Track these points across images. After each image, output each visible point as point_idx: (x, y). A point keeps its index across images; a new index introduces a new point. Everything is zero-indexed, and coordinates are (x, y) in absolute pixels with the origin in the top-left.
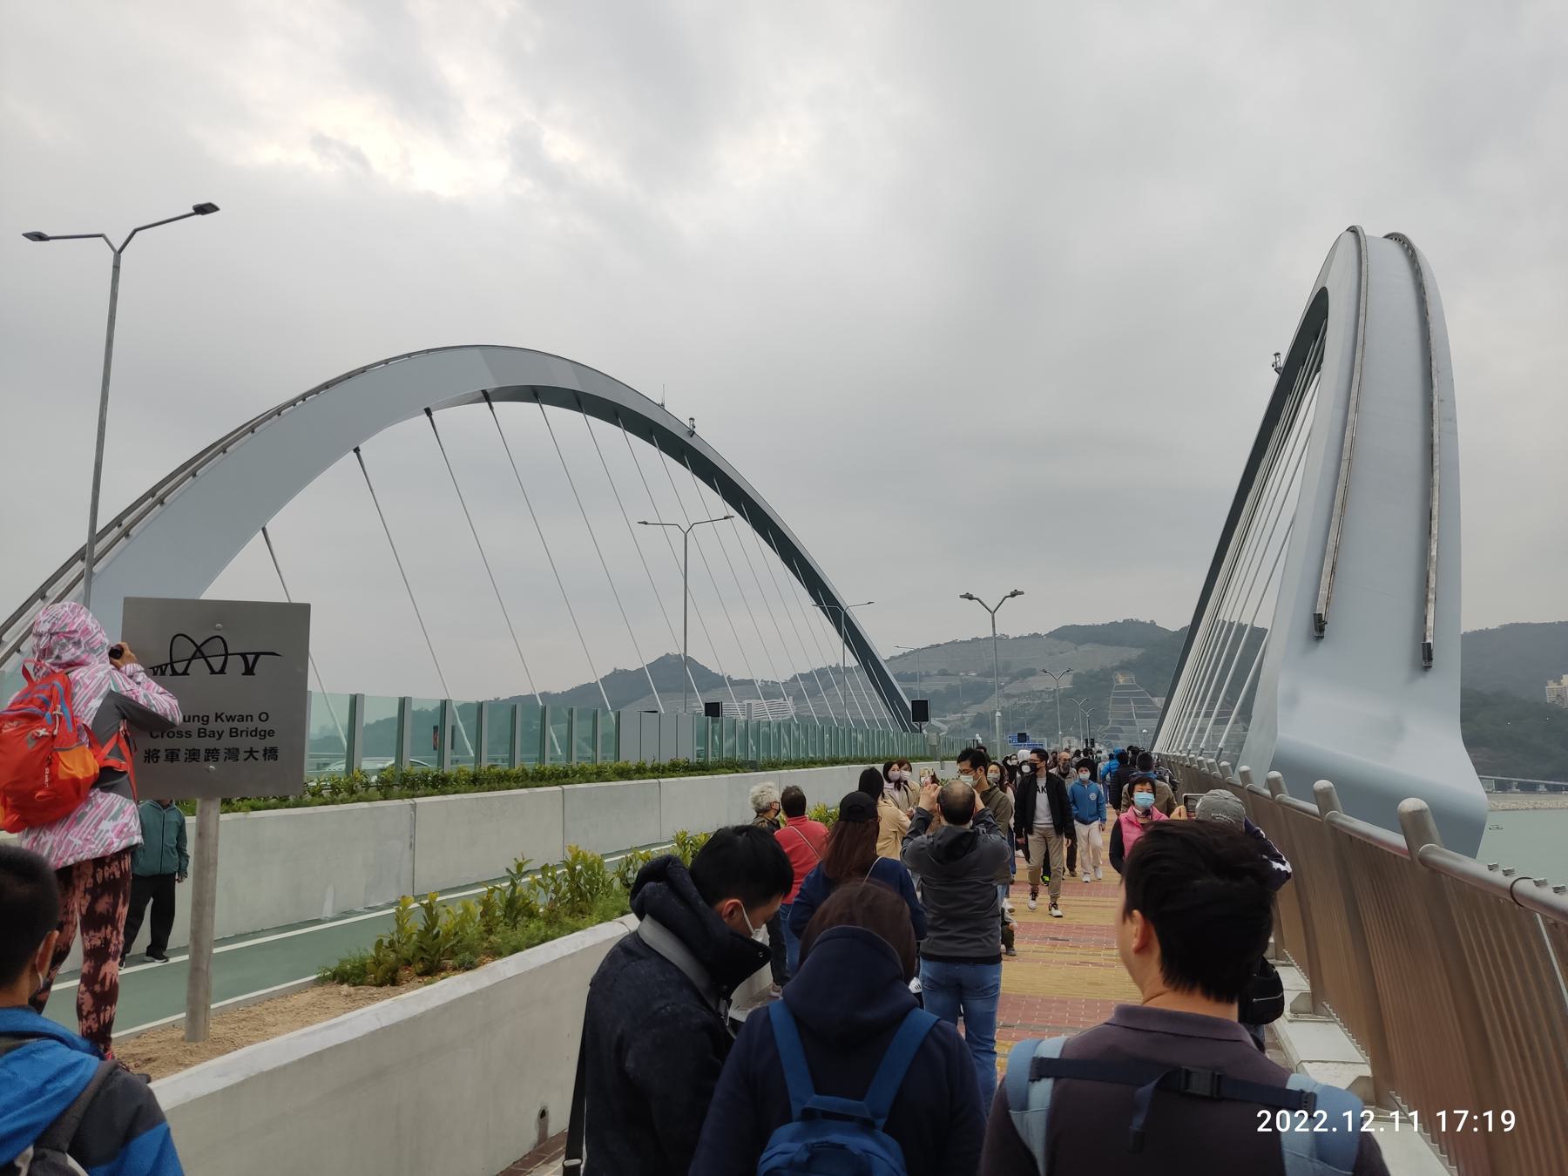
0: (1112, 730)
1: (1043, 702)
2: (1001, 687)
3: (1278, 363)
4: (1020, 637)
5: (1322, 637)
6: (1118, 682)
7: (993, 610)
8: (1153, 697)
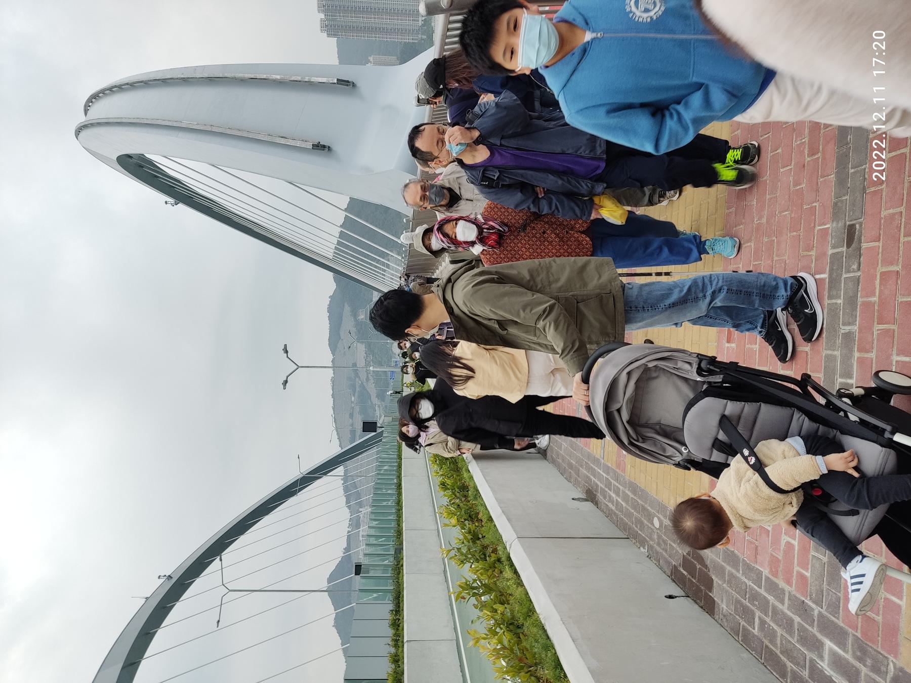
2: (362, 382)
3: (172, 203)
5: (329, 147)
6: (363, 318)
7: (296, 367)
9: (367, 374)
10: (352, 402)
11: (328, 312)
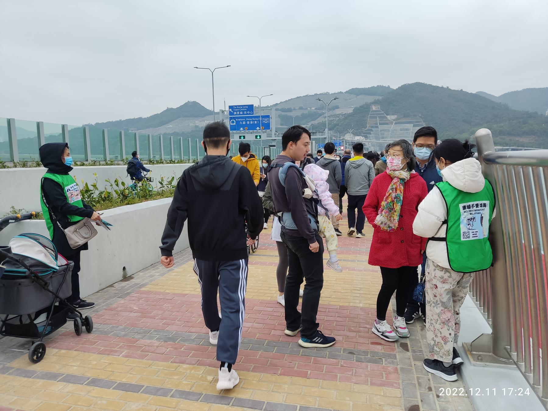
0: (369, 130)
1: (340, 119)
6: (373, 109)
8: (387, 115)
9: (329, 116)
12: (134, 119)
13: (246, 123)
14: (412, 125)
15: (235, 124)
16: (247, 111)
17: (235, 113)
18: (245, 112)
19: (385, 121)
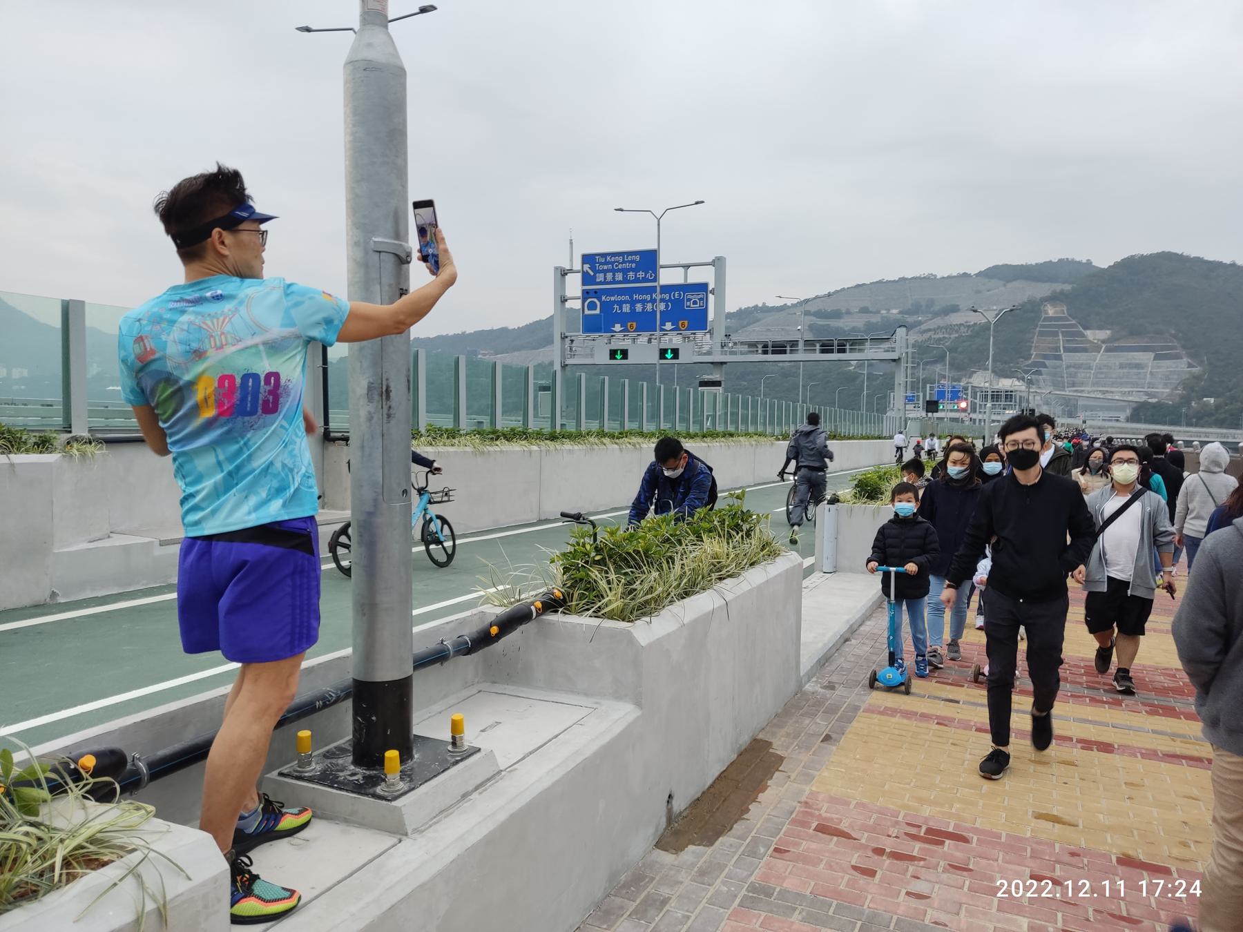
0: (1035, 364)
1: (960, 336)
4: (949, 277)
6: (1047, 313)
8: (1085, 329)
10: (888, 310)
11: (1060, 260)
12: (492, 331)
13: (633, 310)
14: (1152, 355)
15: (597, 311)
16: (635, 270)
17: (600, 277)
18: (631, 274)
19: (1082, 342)
